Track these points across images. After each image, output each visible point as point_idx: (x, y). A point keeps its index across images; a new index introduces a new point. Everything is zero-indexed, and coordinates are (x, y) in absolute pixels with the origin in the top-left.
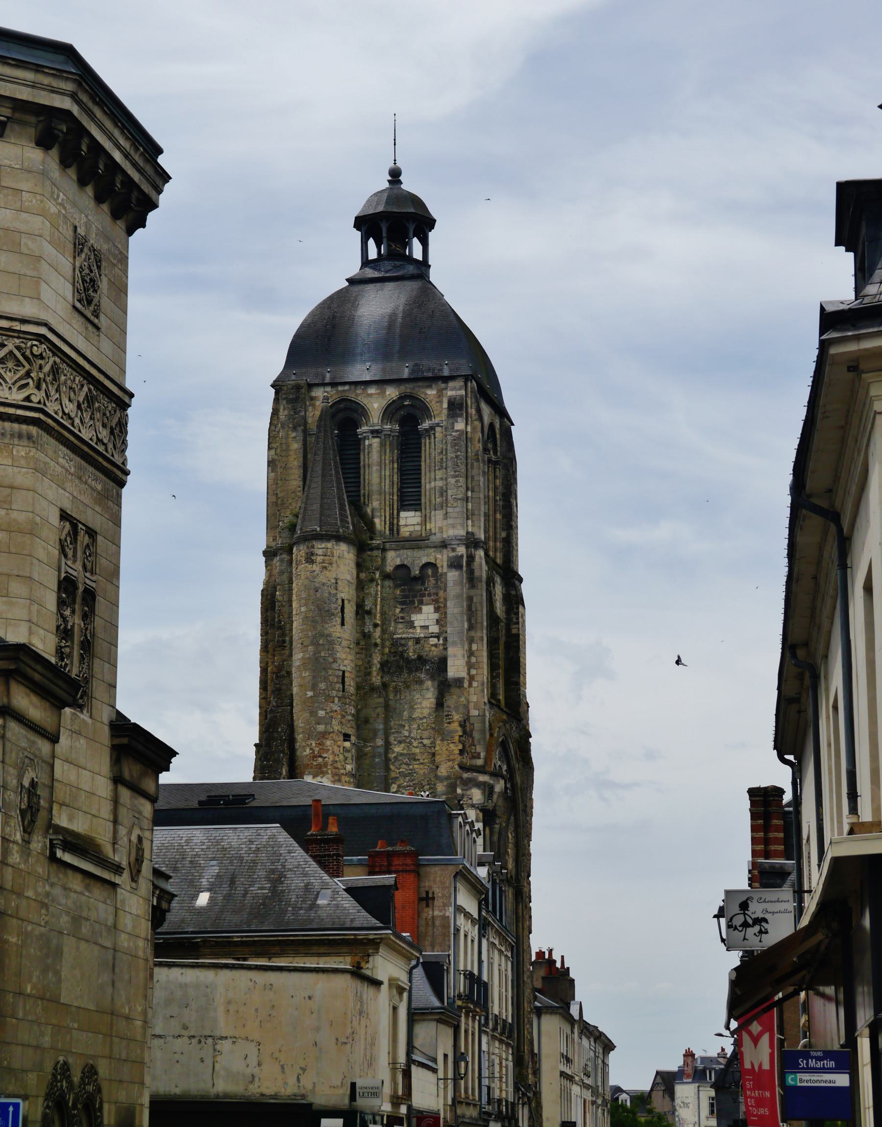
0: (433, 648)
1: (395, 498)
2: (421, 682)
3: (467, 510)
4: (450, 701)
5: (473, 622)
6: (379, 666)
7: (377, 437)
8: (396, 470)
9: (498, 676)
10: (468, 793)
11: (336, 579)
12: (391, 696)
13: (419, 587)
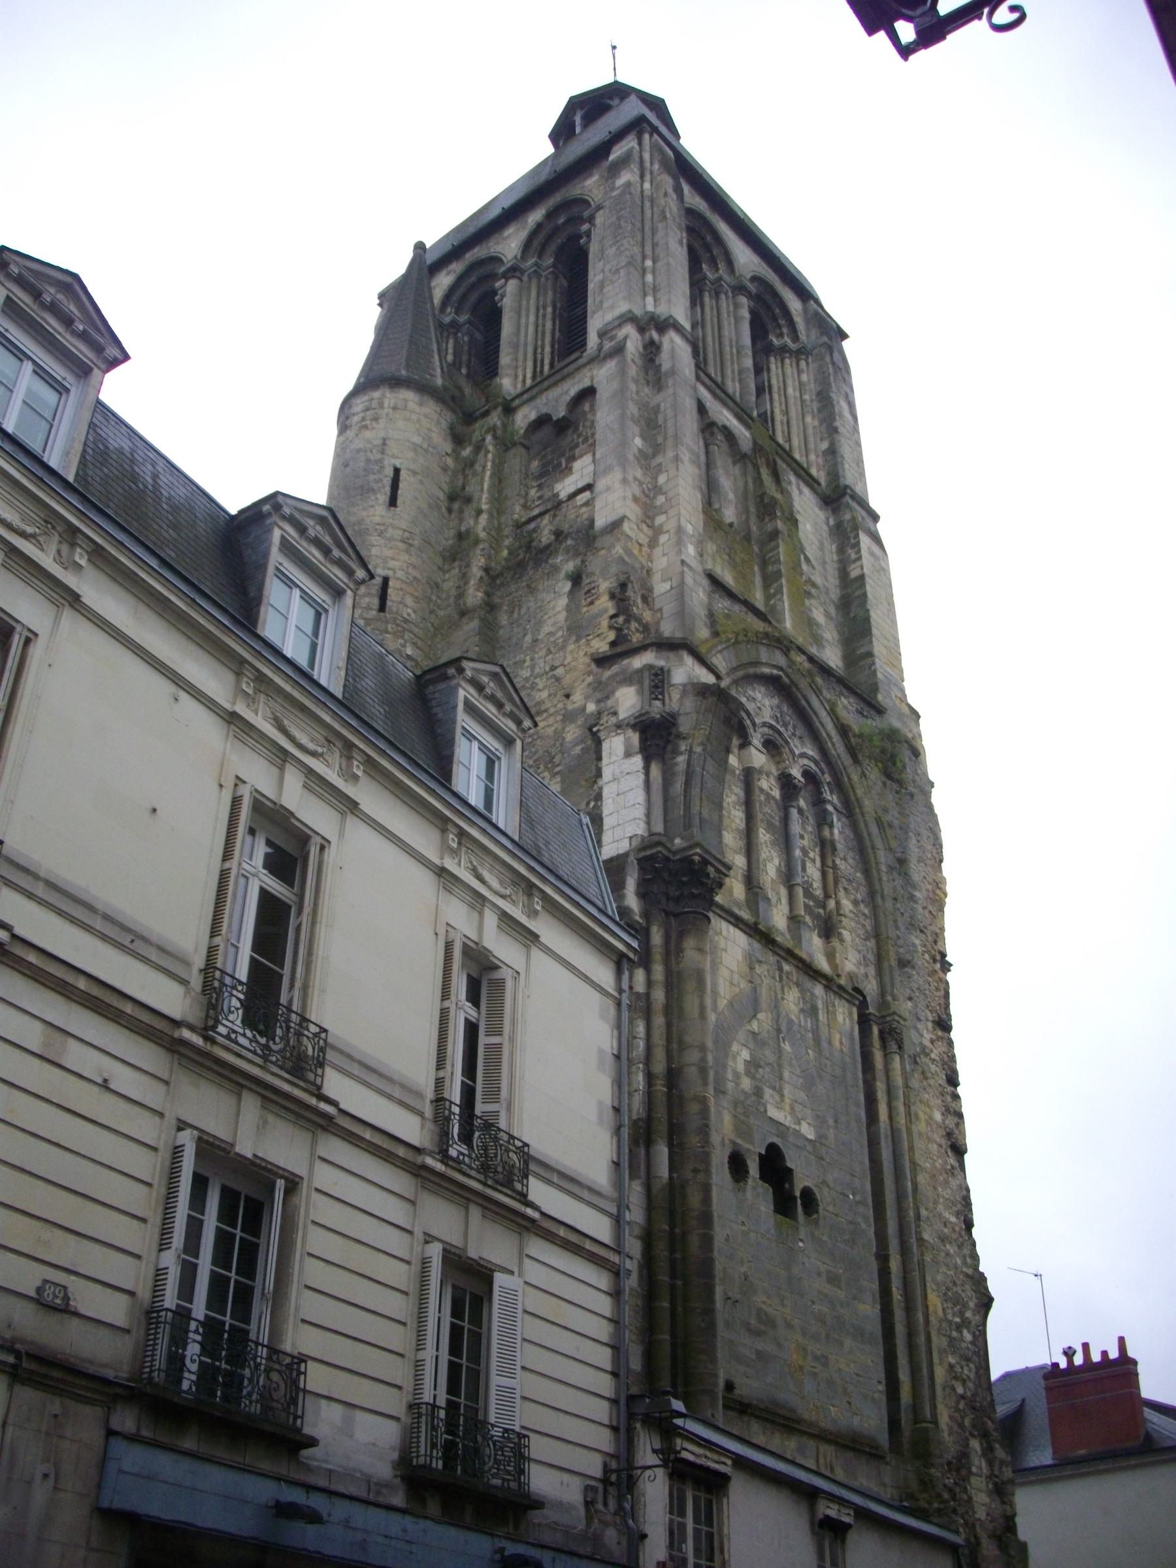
0: (584, 509)
1: (548, 349)
2: (556, 569)
3: (644, 284)
4: (595, 564)
7: (513, 277)
8: (549, 316)
9: (779, 591)
10: (610, 703)
11: (384, 439)
12: (503, 619)
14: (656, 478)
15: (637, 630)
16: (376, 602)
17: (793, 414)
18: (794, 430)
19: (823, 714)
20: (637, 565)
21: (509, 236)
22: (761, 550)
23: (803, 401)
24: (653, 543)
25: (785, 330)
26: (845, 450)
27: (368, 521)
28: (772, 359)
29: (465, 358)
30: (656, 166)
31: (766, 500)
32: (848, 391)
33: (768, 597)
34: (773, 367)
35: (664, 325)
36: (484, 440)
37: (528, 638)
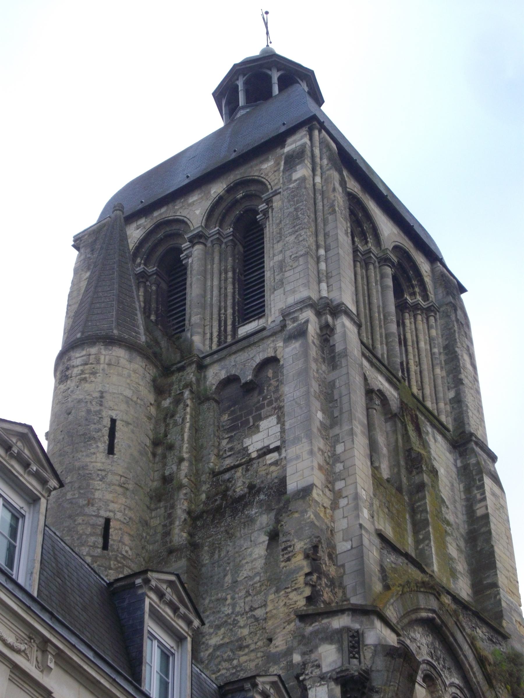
0: (273, 468)
1: (230, 311)
2: (251, 520)
3: (318, 272)
4: (289, 524)
5: (336, 414)
6: (184, 516)
8: (230, 280)
9: (427, 537)
10: (313, 656)
11: (102, 392)
12: (206, 559)
13: (255, 400)
14: (334, 447)
15: (326, 585)
16: (100, 540)
17: (425, 367)
18: (426, 380)
19: (466, 647)
20: (324, 527)
21: (193, 204)
22: (410, 499)
23: (432, 354)
24: (335, 506)
25: (417, 290)
26: (469, 399)
27: (91, 466)
28: (407, 315)
29: (153, 305)
30: (325, 161)
31: (414, 455)
32: (470, 346)
33: (417, 542)
34: (407, 322)
35: (337, 310)
36: (182, 394)
37: (228, 579)
